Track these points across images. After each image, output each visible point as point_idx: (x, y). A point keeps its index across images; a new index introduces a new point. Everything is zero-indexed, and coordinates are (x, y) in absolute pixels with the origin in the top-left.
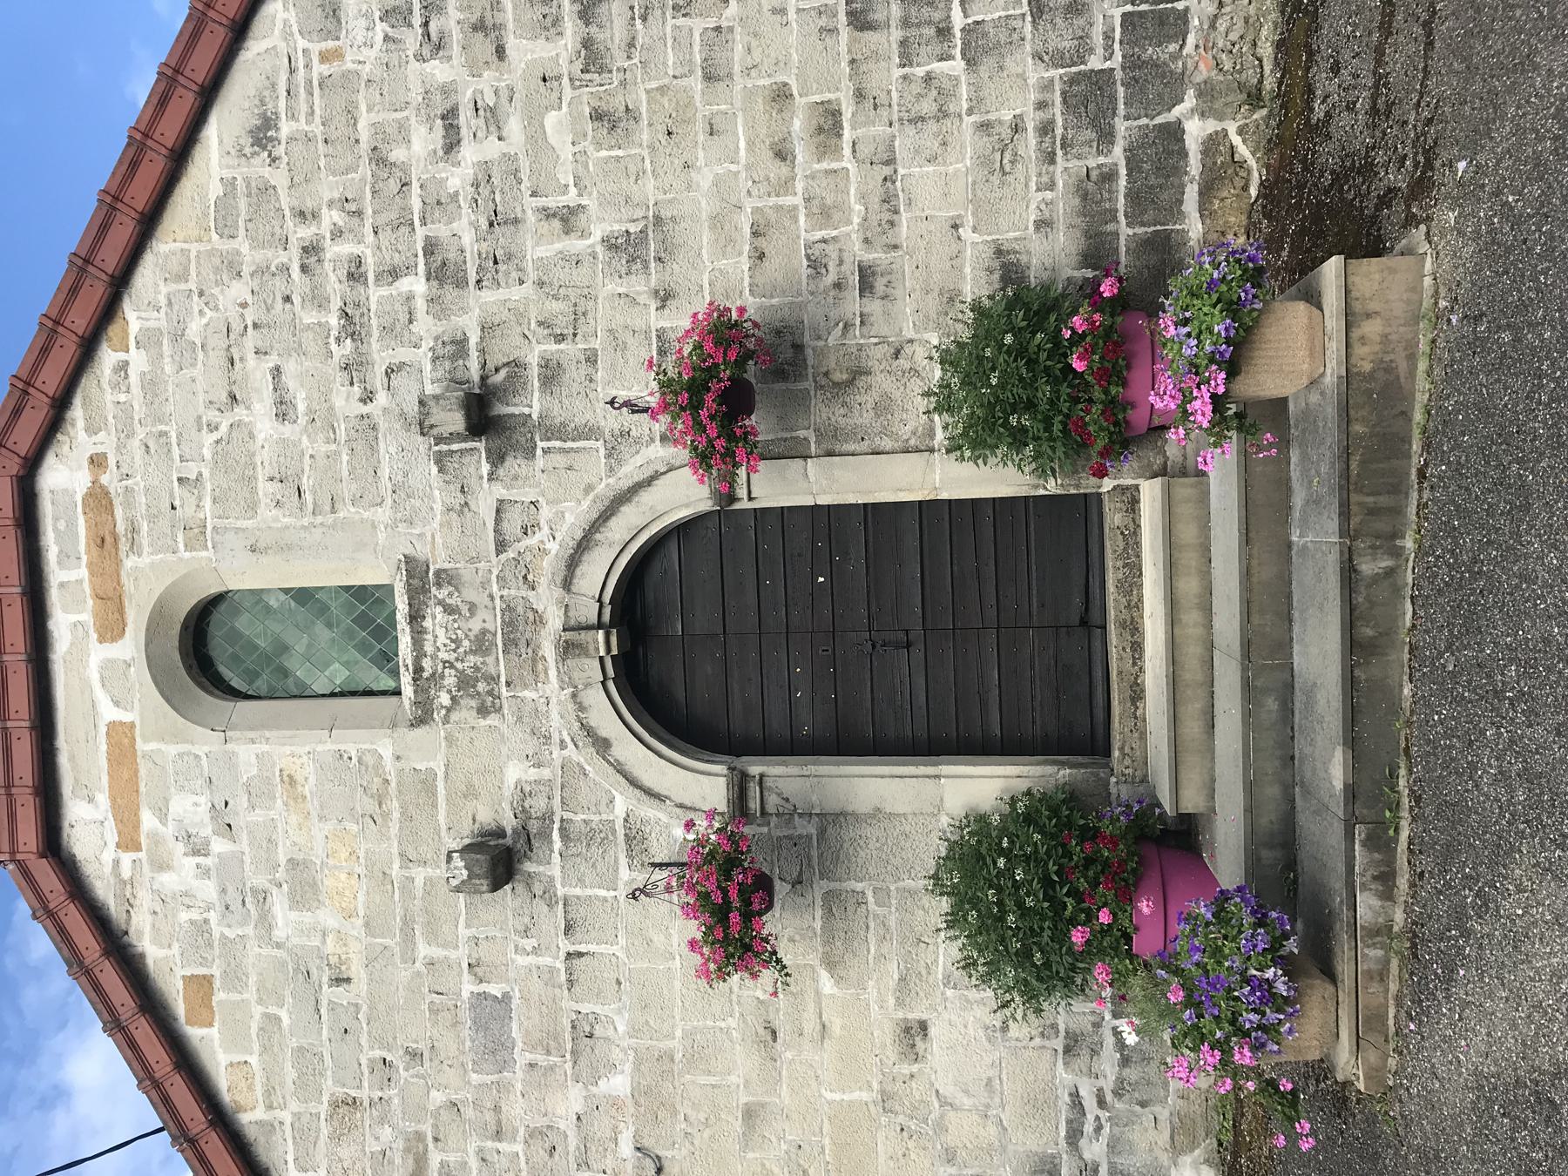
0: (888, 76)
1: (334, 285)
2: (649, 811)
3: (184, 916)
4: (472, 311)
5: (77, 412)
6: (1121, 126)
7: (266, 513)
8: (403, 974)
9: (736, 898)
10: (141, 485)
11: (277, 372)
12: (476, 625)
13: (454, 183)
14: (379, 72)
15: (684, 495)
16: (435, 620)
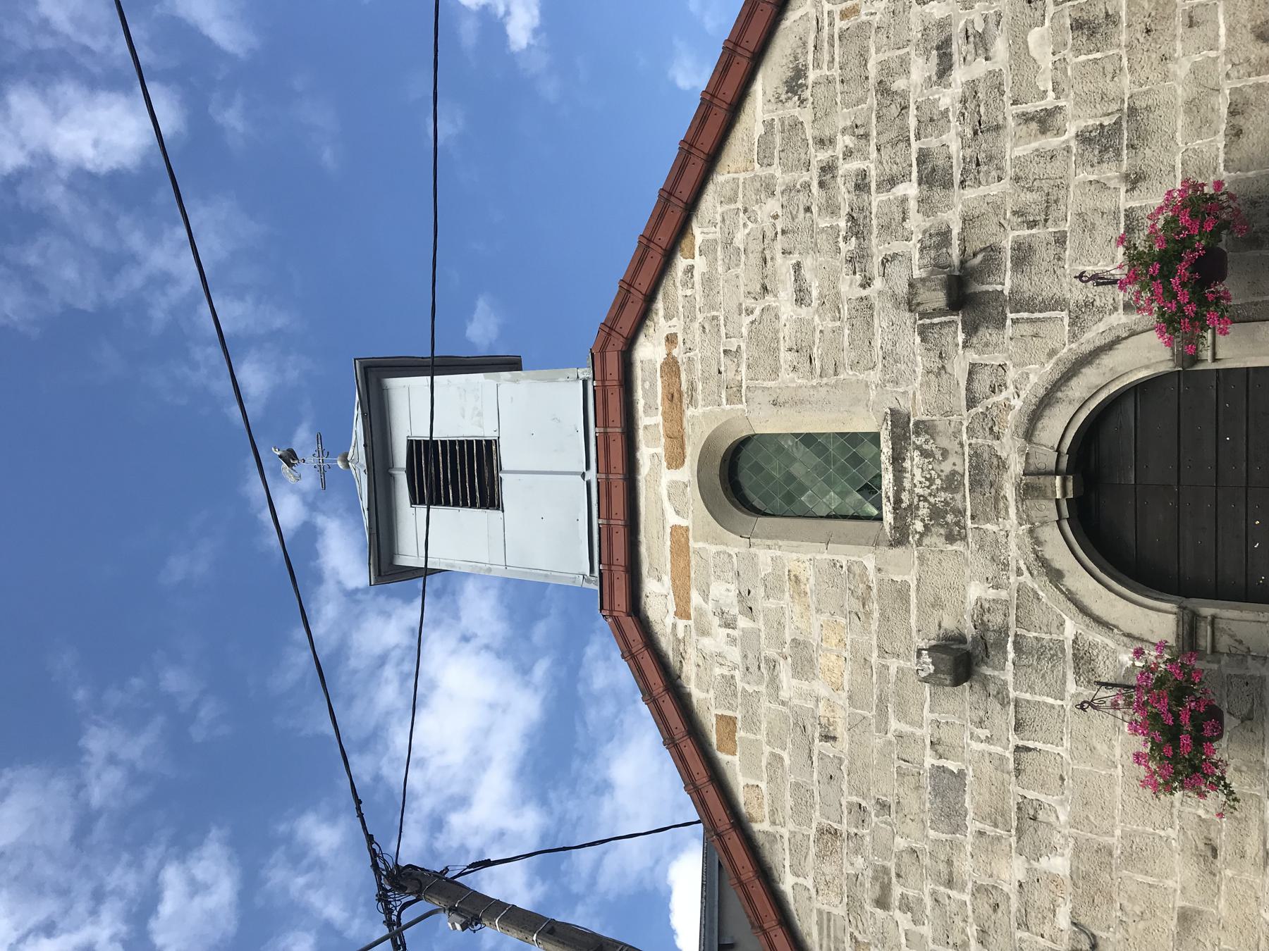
1: (844, 194)
2: (1097, 637)
3: (718, 671)
5: (659, 305)
7: (786, 376)
8: (877, 741)
10: (699, 355)
11: (798, 266)
12: (947, 467)
14: (887, 19)
15: (1146, 355)
16: (913, 462)
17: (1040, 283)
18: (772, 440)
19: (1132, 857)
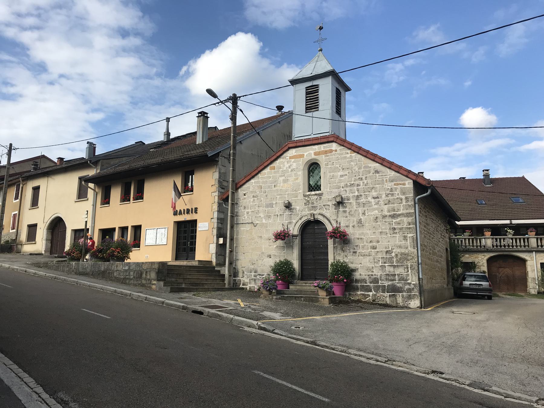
0: (380, 255)
1: (357, 182)
2: (293, 225)
5: (342, 147)
6: (372, 285)
7: (329, 174)
8: (276, 194)
9: (282, 236)
11: (346, 175)
13: (369, 198)
15: (330, 229)
16: (316, 197)
17: (341, 214)
18: (320, 172)
19: (267, 230)
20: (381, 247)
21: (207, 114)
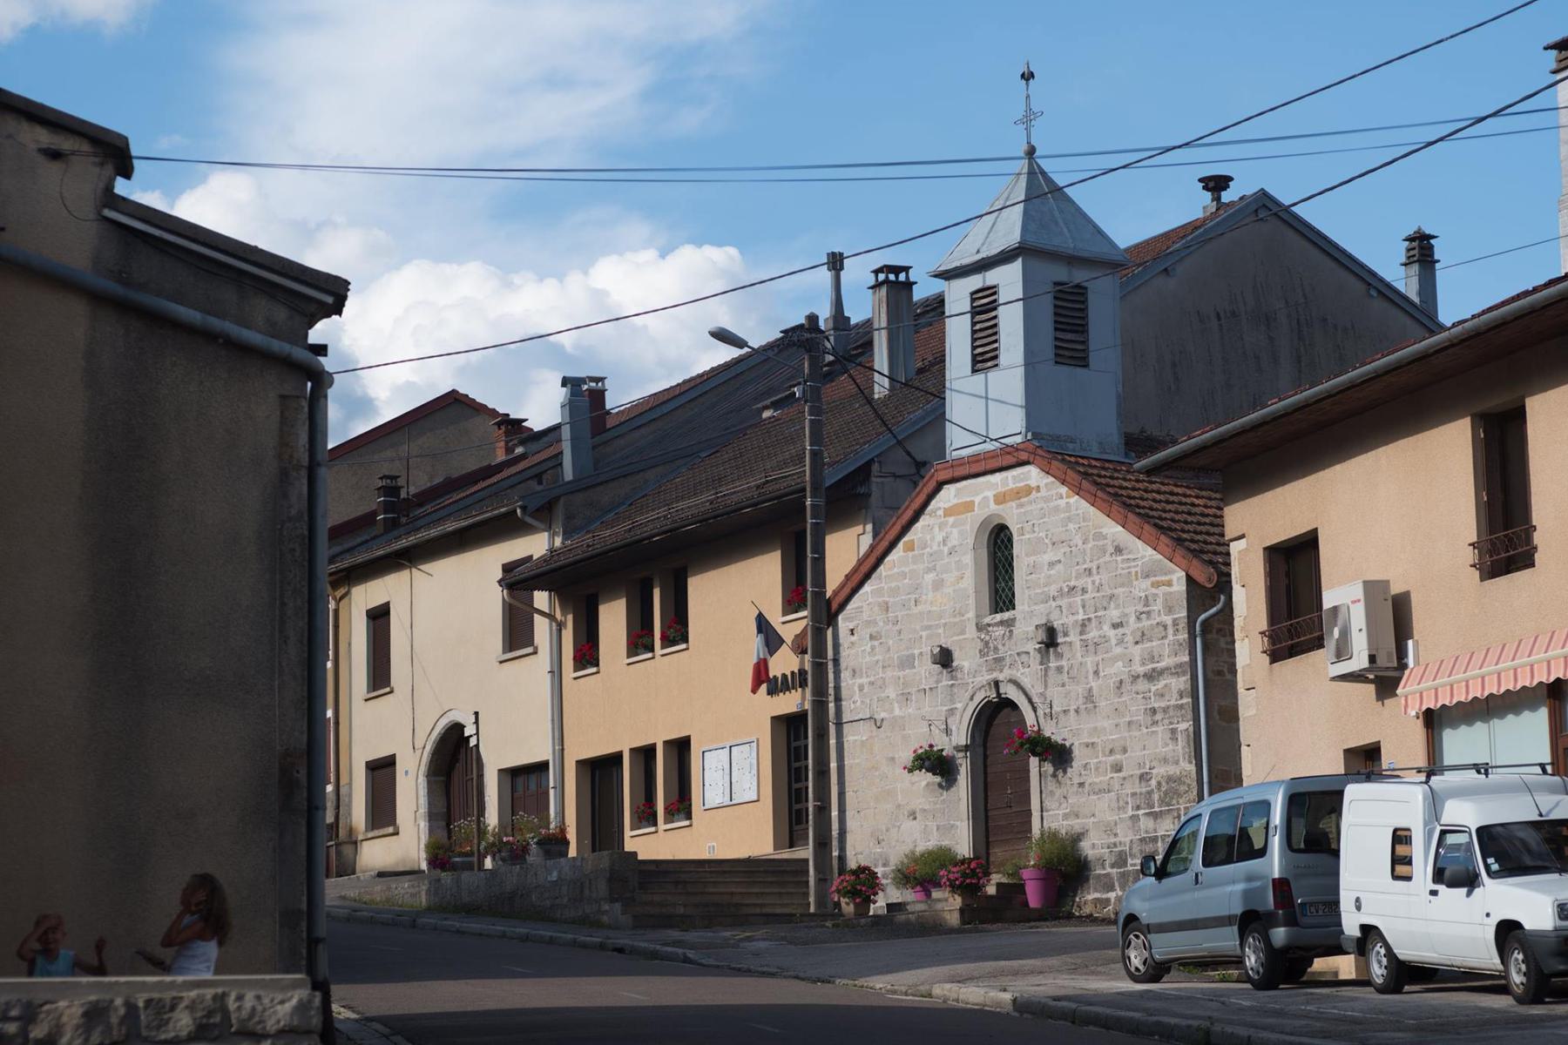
4: (1073, 637)
17: (1053, 677)
20: (1131, 763)
21: (906, 269)
